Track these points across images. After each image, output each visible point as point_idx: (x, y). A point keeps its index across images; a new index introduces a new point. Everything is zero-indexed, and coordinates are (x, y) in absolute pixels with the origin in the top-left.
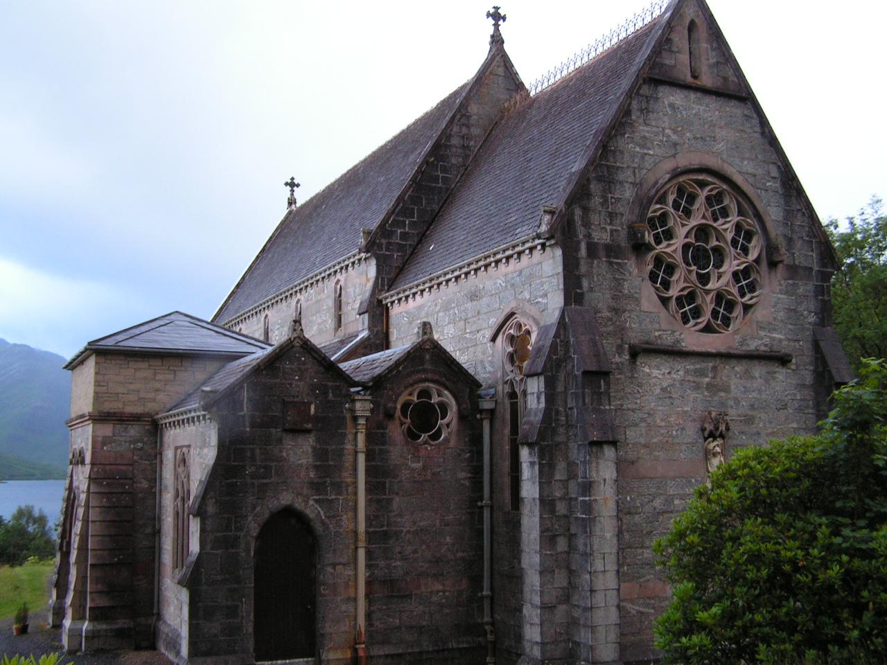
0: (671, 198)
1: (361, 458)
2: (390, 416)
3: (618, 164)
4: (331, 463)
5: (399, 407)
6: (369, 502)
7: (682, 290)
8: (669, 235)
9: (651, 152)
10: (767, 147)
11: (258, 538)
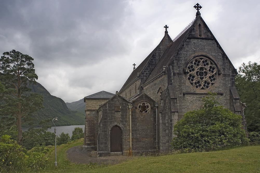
0: (193, 62)
1: (130, 116)
2: (136, 108)
3: (181, 56)
4: (124, 117)
5: (138, 106)
6: (132, 124)
7: (196, 81)
8: (193, 70)
9: (189, 53)
10: (219, 49)
11: (110, 131)
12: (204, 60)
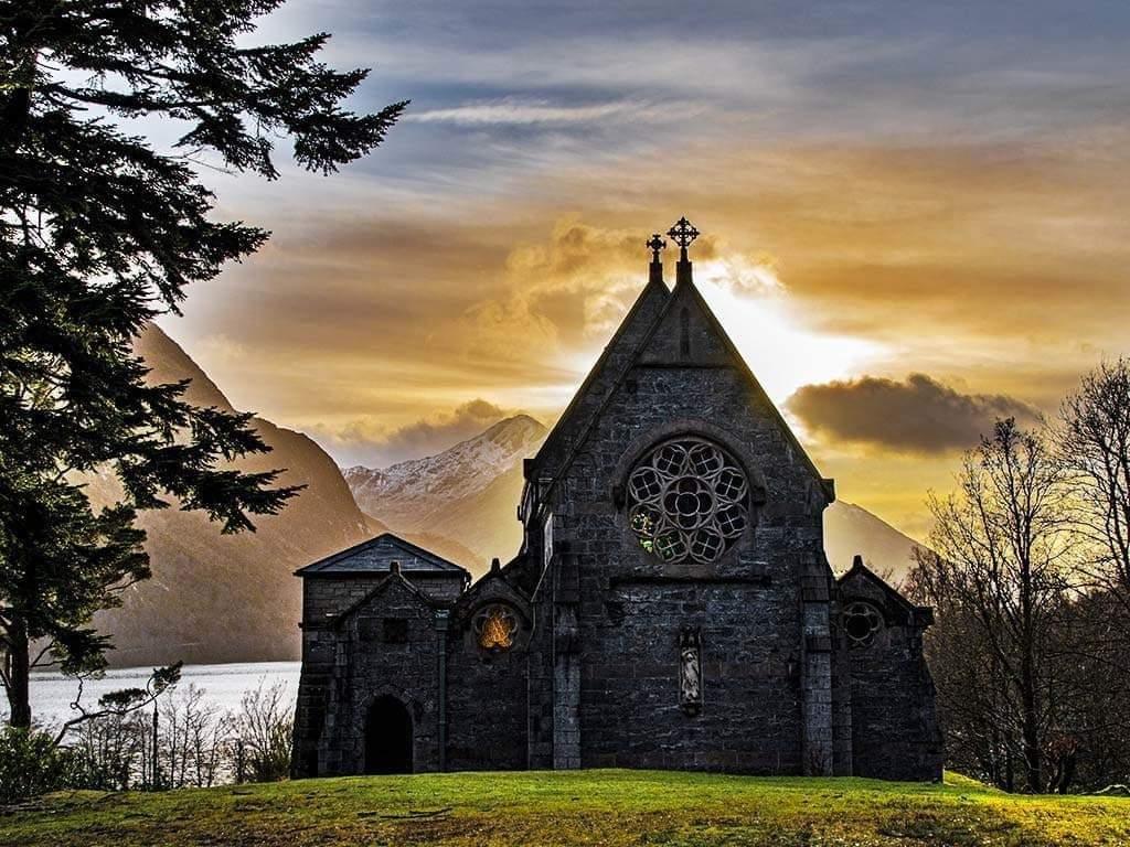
0: (655, 462)
12: (698, 448)
